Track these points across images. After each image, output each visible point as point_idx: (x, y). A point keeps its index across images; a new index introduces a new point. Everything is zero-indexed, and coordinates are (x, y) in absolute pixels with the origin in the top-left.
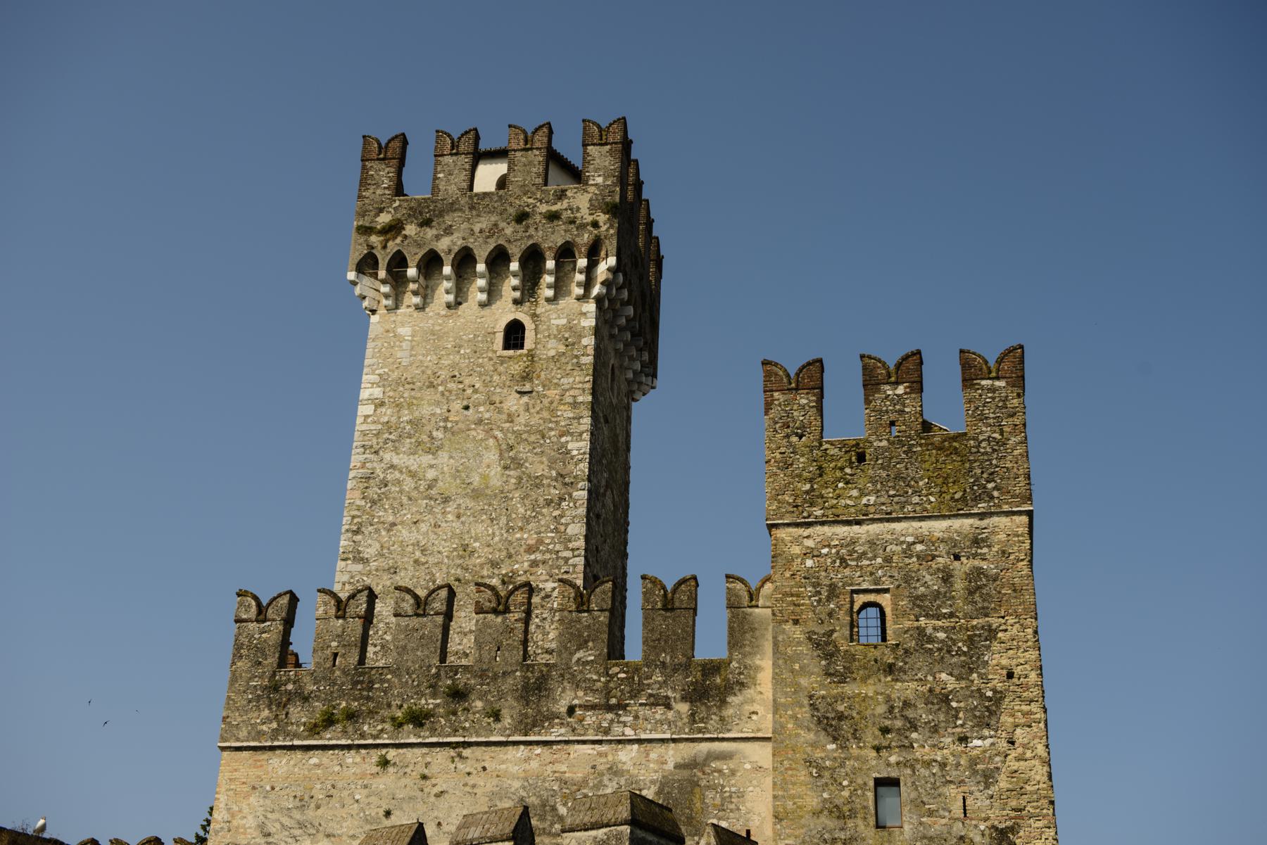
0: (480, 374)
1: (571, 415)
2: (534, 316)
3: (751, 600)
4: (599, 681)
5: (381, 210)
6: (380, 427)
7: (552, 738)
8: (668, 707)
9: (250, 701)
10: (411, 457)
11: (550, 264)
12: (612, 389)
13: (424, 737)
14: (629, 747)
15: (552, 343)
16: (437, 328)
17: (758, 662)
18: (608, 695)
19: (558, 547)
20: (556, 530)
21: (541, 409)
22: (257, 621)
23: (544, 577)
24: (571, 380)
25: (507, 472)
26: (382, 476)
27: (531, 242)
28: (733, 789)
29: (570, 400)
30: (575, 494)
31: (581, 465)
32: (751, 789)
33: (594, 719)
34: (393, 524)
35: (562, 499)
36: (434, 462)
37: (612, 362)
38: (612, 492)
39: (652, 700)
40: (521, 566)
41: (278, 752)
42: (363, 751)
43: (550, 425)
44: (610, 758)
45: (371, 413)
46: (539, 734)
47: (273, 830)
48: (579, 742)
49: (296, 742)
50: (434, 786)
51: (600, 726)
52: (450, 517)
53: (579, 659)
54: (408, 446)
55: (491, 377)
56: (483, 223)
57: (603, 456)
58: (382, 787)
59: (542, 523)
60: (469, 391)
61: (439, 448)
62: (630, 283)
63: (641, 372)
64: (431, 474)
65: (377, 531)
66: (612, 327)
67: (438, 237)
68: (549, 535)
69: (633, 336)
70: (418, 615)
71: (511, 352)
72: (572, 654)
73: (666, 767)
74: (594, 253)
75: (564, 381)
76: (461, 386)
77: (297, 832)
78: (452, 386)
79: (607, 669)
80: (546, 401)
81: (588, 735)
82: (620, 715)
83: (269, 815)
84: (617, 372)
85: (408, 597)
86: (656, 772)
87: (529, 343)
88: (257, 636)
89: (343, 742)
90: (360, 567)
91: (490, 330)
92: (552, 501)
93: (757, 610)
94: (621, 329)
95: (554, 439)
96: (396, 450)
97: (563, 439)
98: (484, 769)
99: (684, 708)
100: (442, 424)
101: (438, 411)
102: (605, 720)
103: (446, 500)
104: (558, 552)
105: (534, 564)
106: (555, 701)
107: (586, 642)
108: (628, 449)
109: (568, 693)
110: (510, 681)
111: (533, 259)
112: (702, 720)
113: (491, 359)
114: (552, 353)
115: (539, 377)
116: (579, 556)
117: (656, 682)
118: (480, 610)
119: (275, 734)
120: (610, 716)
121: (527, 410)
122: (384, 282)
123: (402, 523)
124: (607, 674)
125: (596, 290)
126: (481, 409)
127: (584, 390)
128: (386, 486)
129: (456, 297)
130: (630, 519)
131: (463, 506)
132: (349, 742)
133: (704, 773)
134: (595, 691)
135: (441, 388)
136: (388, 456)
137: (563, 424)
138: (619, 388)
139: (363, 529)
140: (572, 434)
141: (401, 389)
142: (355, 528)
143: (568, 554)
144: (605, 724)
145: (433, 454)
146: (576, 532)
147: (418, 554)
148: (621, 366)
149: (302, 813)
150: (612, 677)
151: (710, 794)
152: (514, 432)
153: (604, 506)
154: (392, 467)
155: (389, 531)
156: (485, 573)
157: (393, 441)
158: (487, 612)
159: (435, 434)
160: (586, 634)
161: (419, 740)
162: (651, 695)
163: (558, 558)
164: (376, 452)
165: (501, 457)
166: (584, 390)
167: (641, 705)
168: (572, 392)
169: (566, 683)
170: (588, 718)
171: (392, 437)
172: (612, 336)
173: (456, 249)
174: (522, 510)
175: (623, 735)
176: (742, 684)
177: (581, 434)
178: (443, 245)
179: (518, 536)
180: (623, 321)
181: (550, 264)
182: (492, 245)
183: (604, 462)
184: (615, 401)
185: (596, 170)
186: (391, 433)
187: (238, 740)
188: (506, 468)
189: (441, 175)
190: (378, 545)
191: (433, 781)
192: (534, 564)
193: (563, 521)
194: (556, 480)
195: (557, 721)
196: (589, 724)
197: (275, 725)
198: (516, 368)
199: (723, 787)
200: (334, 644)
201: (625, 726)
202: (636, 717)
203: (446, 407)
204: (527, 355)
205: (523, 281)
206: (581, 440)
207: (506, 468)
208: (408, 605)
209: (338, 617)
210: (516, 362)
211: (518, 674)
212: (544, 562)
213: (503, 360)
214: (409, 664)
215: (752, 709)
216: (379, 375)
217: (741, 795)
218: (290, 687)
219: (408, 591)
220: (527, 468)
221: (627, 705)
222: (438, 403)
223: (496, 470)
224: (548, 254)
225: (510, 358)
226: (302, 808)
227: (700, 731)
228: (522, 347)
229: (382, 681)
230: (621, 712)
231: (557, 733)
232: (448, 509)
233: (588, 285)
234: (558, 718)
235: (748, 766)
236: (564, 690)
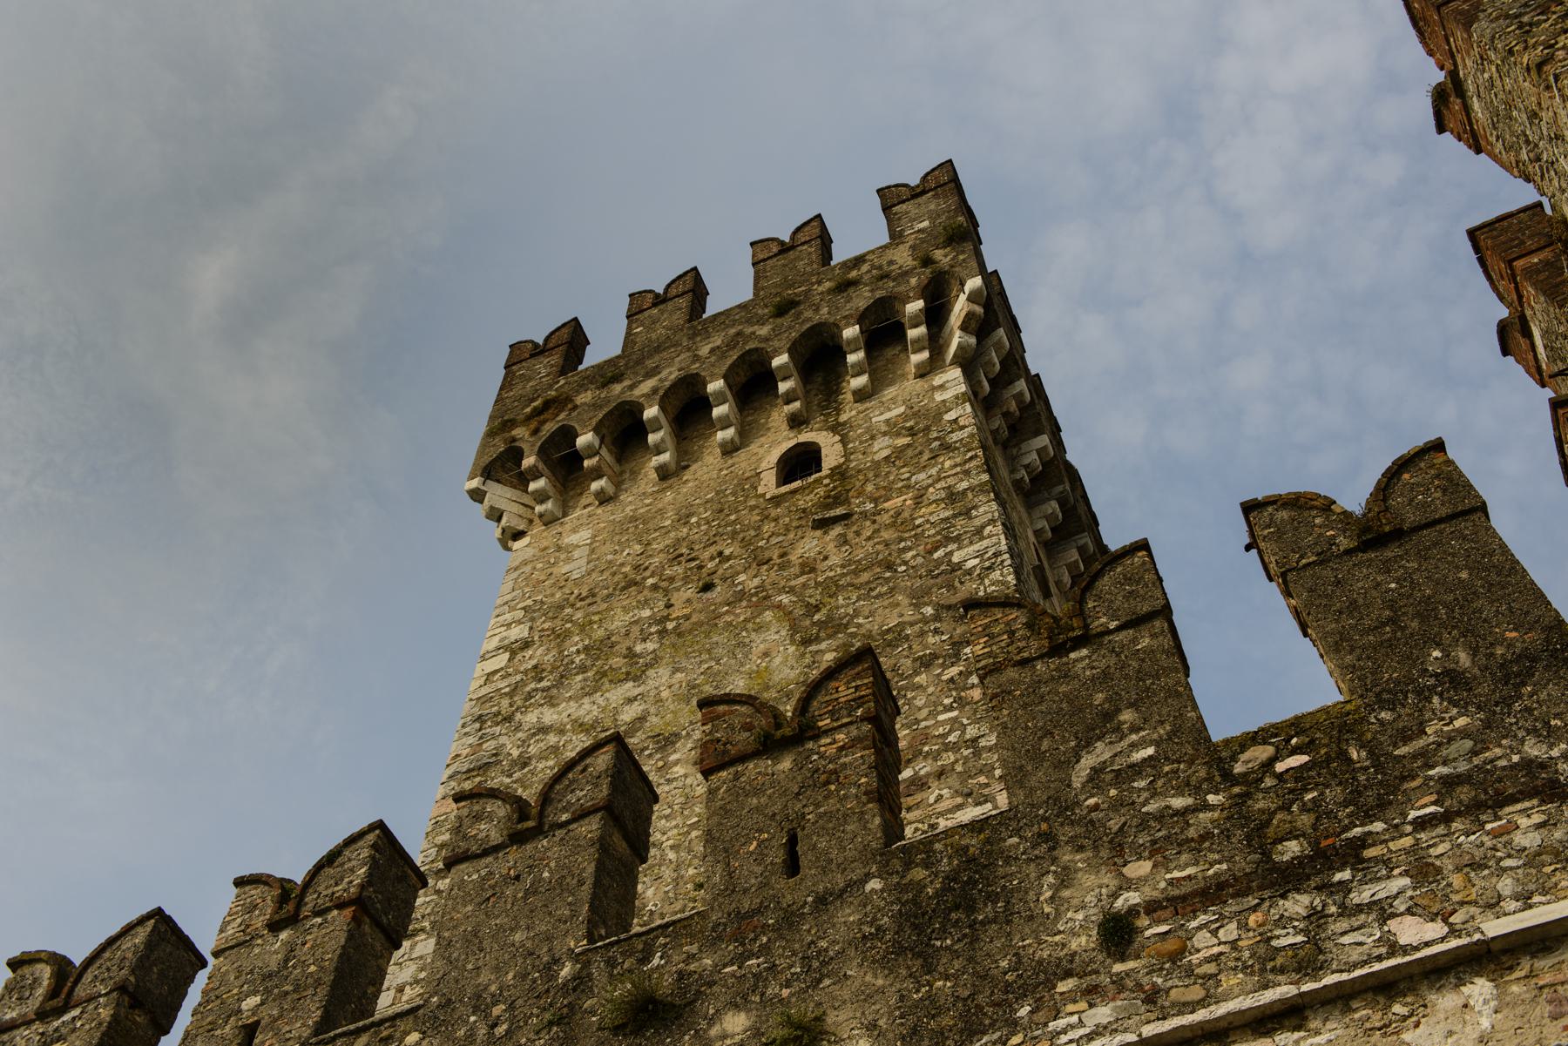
4: (1206, 807)
10: (586, 700)
14: (1446, 1001)
18: (1260, 836)
31: (996, 575)
39: (1465, 793)
53: (1097, 771)
68: (941, 718)
72: (1067, 763)
81: (1225, 998)
82: (1345, 887)
102: (1282, 921)
104: (975, 740)
106: (1044, 924)
107: (1109, 716)
109: (1088, 880)
110: (848, 915)
120: (1298, 904)
124: (1229, 778)
140: (957, 539)
144: (1288, 939)
150: (1251, 781)
154: (543, 730)
158: (743, 758)
163: (977, 753)
167: (1422, 824)
169: (1066, 856)
170: (1202, 939)
175: (1394, 948)
188: (806, 642)
195: (1063, 987)
196: (1215, 958)
201: (1385, 917)
202: (1423, 871)
211: (875, 884)
212: (940, 774)
214: (484, 978)
216: (524, 608)
220: (859, 626)
221: (1363, 842)
230: (1345, 875)
232: (673, 757)
233: (935, 342)
234: (1068, 974)
236: (1066, 878)
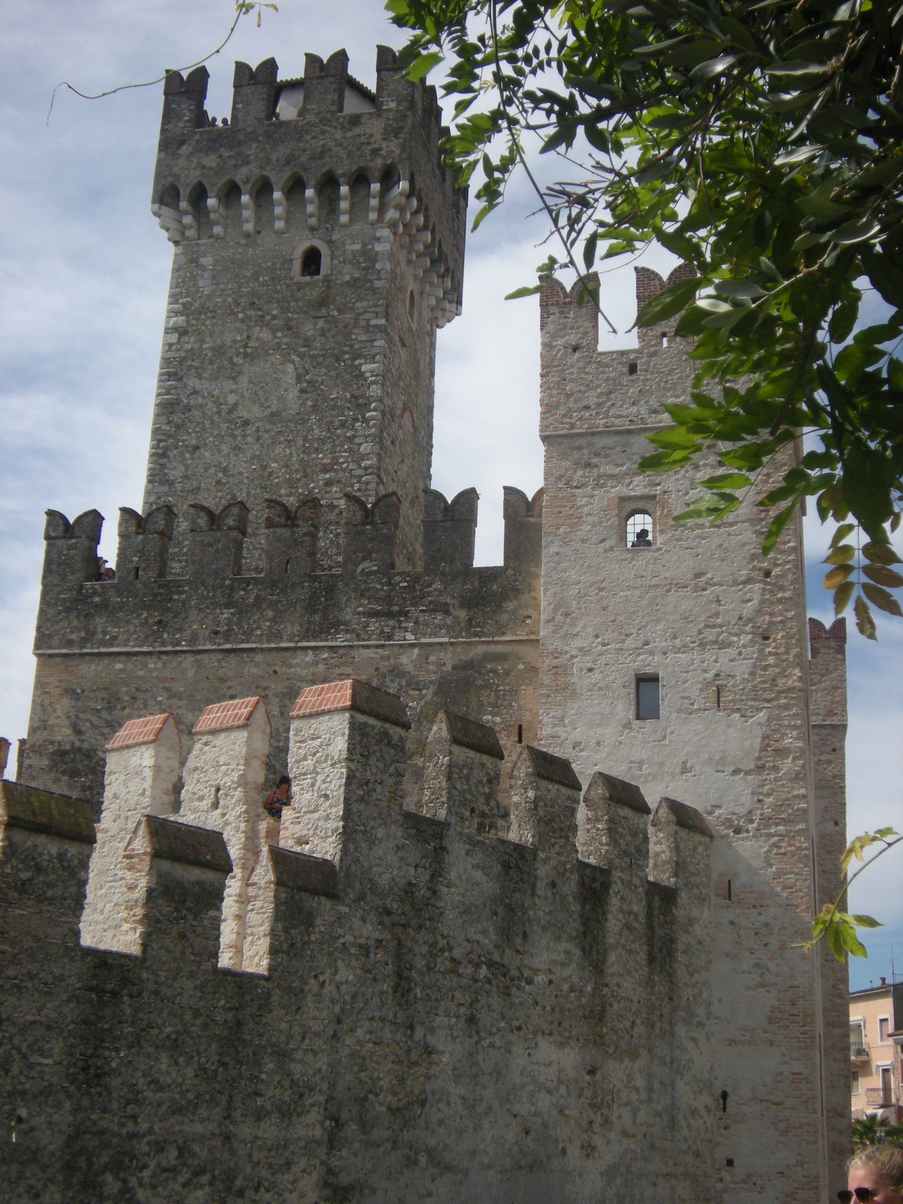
0: (278, 302)
1: (364, 338)
2: (330, 243)
3: (528, 510)
5: (182, 143)
6: (183, 354)
7: (338, 644)
8: (447, 612)
9: (60, 613)
11: (344, 189)
12: (411, 315)
13: (219, 644)
15: (347, 269)
16: (237, 257)
17: (533, 569)
19: (351, 467)
20: (350, 450)
21: (337, 333)
22: (65, 538)
23: (337, 496)
24: (365, 304)
25: (305, 396)
26: (185, 401)
27: (325, 169)
28: (507, 688)
29: (363, 323)
30: (368, 415)
32: (524, 687)
33: (377, 625)
34: (196, 448)
35: (356, 420)
36: (233, 387)
37: (411, 287)
38: (412, 414)
40: (316, 487)
41: (87, 658)
42: (164, 657)
43: (345, 348)
44: (392, 661)
45: (176, 341)
46: (327, 640)
47: (84, 729)
48: (363, 646)
49: (103, 650)
50: (229, 688)
51: (382, 632)
52: (249, 439)
53: (363, 570)
54: (210, 372)
55: (289, 303)
56: (280, 153)
57: (400, 378)
58: (182, 689)
59: (337, 443)
60: (268, 318)
61: (240, 373)
62: (427, 209)
63: (444, 298)
64: (232, 399)
65: (182, 454)
66: (409, 252)
67: (236, 167)
69: (433, 262)
70: (211, 530)
71: (308, 279)
72: (356, 565)
73: (444, 669)
74: (388, 177)
75: (358, 305)
76: (260, 313)
77: (106, 731)
78: (251, 313)
79: (390, 579)
80: (341, 326)
83: (81, 716)
84: (417, 298)
85: (202, 514)
86: (434, 673)
87: (324, 269)
88: (65, 552)
89: (145, 649)
90: (165, 488)
91: (288, 257)
92: (346, 421)
93: (532, 519)
94: (419, 256)
95: (349, 362)
96: (200, 377)
97: (357, 362)
98: (275, 672)
99: (462, 614)
100: (242, 350)
101: (239, 338)
103: (246, 423)
105: (329, 483)
106: (341, 610)
107: (370, 553)
108: (432, 374)
109: (353, 601)
111: (328, 184)
112: (478, 625)
113: (288, 286)
114: (347, 278)
115: (334, 301)
116: (371, 474)
117: (436, 590)
118: (270, 524)
119: (83, 642)
120: (391, 623)
121: (323, 335)
122: (186, 213)
123: (206, 445)
124: (389, 583)
125: (392, 214)
126: (279, 334)
127: (377, 313)
128: (190, 410)
129: (256, 226)
130: (434, 442)
131: (262, 429)
132: (151, 649)
133: (480, 673)
134: (377, 600)
135: (241, 316)
136: (192, 382)
137: (357, 346)
138: (420, 314)
139: (169, 453)
140: (365, 357)
141: (203, 317)
142: (160, 451)
143: (358, 472)
144: (387, 630)
145: (234, 379)
146: (368, 451)
147: (220, 475)
148: (422, 293)
149: (110, 714)
151: (484, 693)
152: (310, 356)
153: (400, 427)
154: (195, 392)
155: (192, 454)
156: (283, 492)
157: (196, 368)
158: (277, 527)
159: (235, 360)
160: (369, 546)
161: (215, 647)
162: (430, 602)
164: (180, 379)
165: (299, 379)
166: (377, 313)
167: (422, 611)
168: (366, 316)
171: (194, 364)
172: (409, 262)
173: (253, 179)
174: (317, 431)
175: (405, 639)
176: (517, 591)
177: (374, 356)
178: (240, 176)
179: (314, 456)
180: (420, 247)
181: (344, 189)
182: (287, 173)
183: (402, 384)
184: (414, 326)
185: (388, 96)
186: (193, 360)
187: (50, 647)
189: (240, 106)
190: (183, 468)
191: (229, 684)
192: (329, 483)
193: (357, 441)
194: (350, 402)
197: (83, 634)
198: (314, 294)
199: (498, 686)
200: (136, 559)
201: (406, 631)
202: (417, 622)
203: (245, 335)
204: (323, 281)
205: (320, 207)
206: (374, 362)
207: (303, 391)
208: (203, 521)
209: (138, 533)
210: (313, 288)
211: (306, 584)
212: (338, 482)
213: (300, 286)
215: (526, 613)
216: (183, 304)
217: (514, 692)
218: (97, 599)
219: (203, 508)
221: (408, 611)
222: (239, 331)
223: (293, 393)
224: (341, 180)
225: (307, 284)
226: (110, 709)
227: (476, 635)
228: (317, 272)
229: (180, 593)
231: (340, 640)
233: (382, 210)
235: (521, 667)
236: (349, 599)
